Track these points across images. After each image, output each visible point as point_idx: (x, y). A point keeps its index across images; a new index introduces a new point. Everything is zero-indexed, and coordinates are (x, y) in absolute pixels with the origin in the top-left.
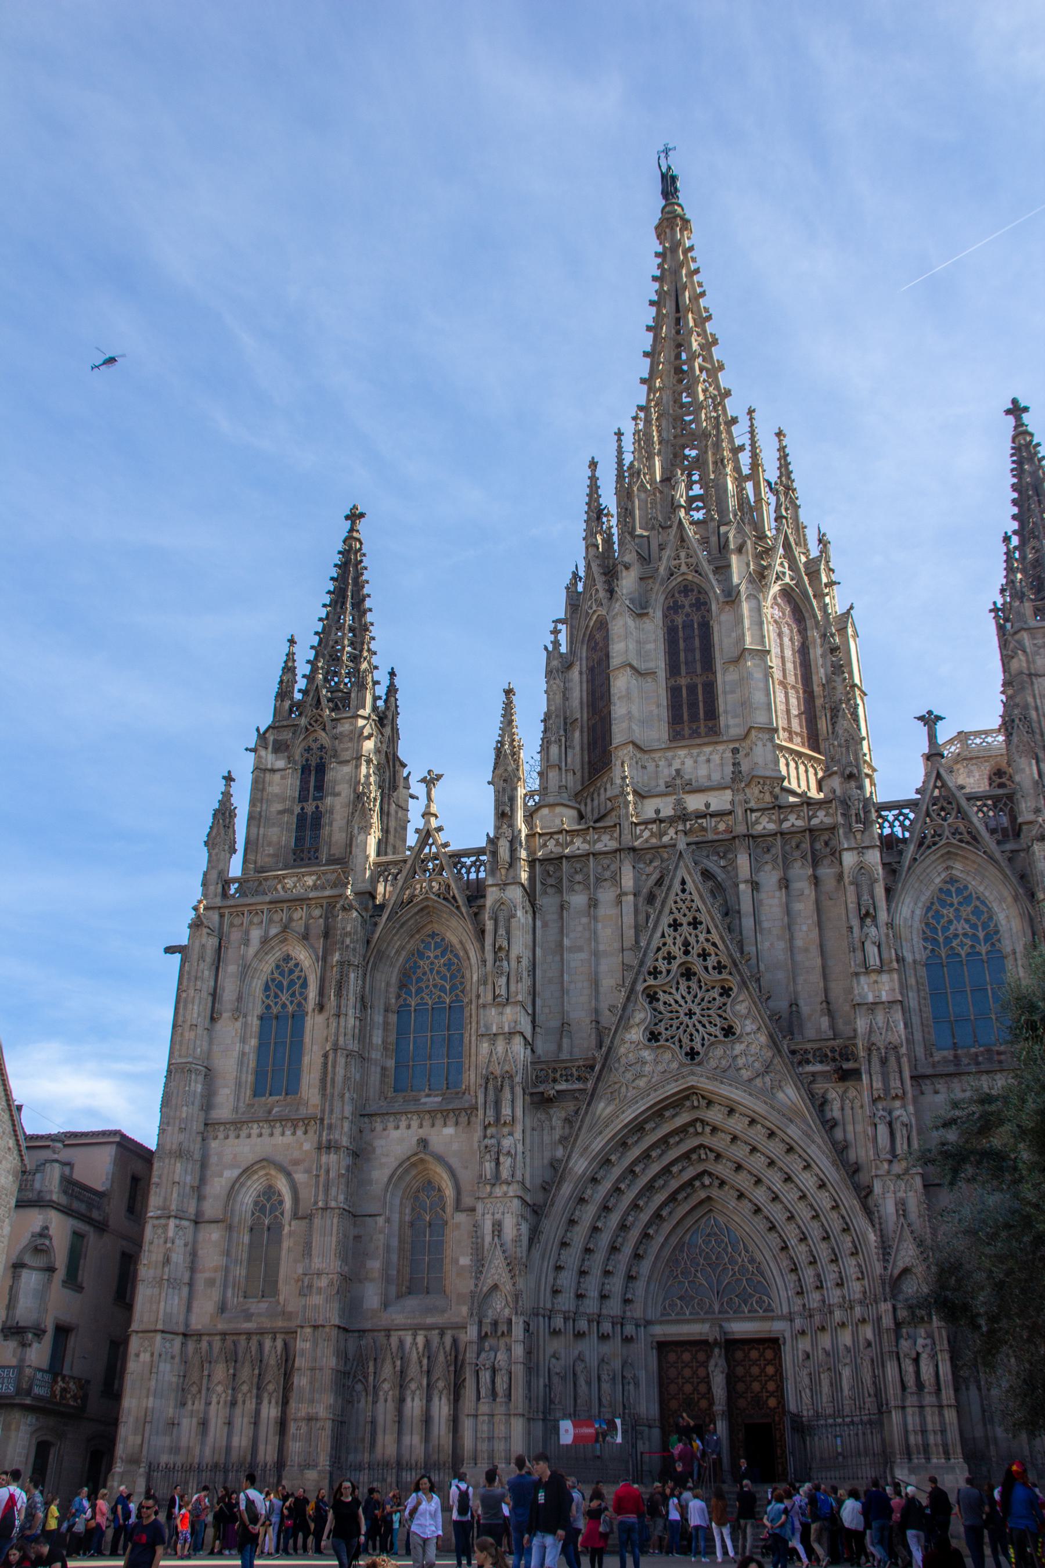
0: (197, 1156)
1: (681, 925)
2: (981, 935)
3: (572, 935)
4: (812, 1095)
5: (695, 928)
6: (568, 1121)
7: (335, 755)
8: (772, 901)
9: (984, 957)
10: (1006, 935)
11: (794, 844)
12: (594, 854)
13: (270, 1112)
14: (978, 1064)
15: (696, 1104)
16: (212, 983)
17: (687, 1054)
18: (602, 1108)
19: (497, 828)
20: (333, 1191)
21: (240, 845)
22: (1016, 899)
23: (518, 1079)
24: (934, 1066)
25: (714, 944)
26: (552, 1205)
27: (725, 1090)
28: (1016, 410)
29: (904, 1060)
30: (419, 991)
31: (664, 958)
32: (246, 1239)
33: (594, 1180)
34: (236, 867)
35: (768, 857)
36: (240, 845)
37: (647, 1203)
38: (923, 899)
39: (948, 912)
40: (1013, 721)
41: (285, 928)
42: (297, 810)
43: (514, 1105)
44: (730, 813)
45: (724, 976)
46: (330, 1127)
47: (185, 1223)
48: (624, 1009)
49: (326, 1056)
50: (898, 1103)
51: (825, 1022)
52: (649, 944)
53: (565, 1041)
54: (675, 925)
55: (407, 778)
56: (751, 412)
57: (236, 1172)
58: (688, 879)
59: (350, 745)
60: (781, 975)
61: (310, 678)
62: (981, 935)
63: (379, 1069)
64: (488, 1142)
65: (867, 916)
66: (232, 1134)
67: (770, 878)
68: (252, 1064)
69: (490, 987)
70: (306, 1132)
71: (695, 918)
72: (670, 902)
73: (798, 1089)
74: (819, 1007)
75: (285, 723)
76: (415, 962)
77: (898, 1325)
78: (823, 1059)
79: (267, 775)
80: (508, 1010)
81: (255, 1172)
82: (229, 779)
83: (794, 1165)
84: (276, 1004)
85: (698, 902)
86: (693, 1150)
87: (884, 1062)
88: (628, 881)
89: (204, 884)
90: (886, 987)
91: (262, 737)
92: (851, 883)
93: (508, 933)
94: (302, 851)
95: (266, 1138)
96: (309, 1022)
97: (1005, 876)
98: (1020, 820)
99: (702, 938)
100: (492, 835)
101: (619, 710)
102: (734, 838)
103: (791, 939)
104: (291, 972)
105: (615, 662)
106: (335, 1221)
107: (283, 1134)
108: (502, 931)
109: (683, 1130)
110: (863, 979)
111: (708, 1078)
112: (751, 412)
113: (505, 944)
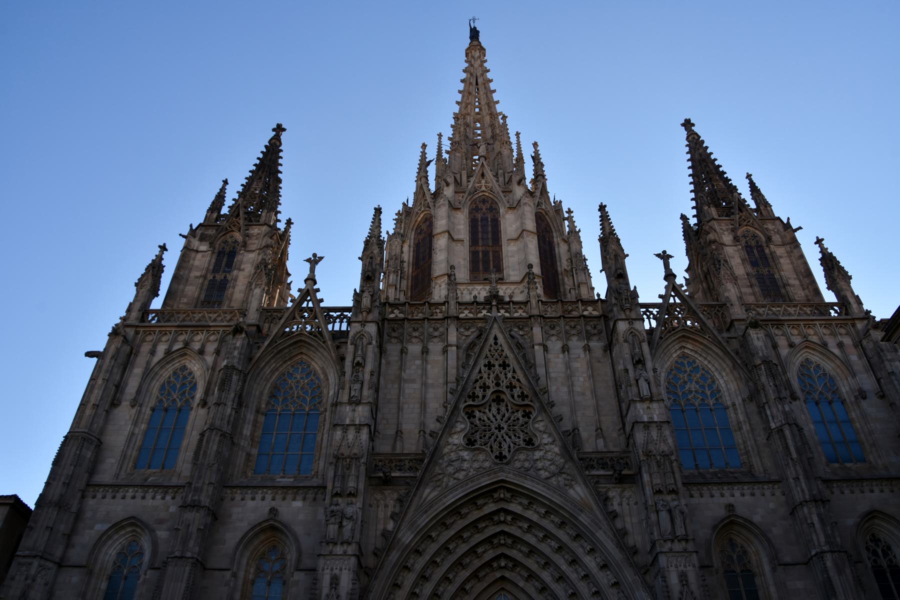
0: (74, 509)
1: (494, 366)
2: (709, 393)
3: (407, 371)
4: (598, 494)
5: (505, 369)
6: (400, 501)
7: (245, 245)
8: (557, 361)
9: (713, 408)
10: (726, 394)
11: (572, 324)
13: (146, 480)
14: (719, 478)
15: (502, 496)
16: (118, 378)
17: (496, 457)
18: (429, 493)
19: (362, 286)
20: (191, 543)
22: (734, 366)
23: (363, 460)
25: (518, 380)
26: (381, 568)
27: (528, 484)
28: (688, 124)
29: (675, 464)
30: (285, 399)
31: (481, 387)
32: (104, 586)
33: (418, 552)
34: (157, 304)
35: (553, 332)
37: (455, 577)
38: (666, 366)
39: (684, 377)
40: (719, 261)
41: (187, 344)
42: (210, 277)
43: (356, 481)
44: (526, 303)
45: (526, 402)
46: (198, 490)
47: (50, 565)
48: (449, 419)
49: (202, 435)
50: (674, 496)
52: (469, 376)
53: (398, 443)
56: (518, 134)
57: (106, 526)
61: (234, 209)
62: (709, 393)
63: (244, 454)
64: (334, 508)
65: (639, 362)
66: (109, 495)
67: (555, 345)
68: (138, 443)
69: (347, 391)
70: (173, 498)
71: (504, 362)
72: (486, 351)
73: (587, 487)
74: (594, 433)
78: (604, 466)
79: (193, 254)
80: (360, 408)
81: (123, 527)
82: (163, 248)
83: (578, 549)
84: (168, 400)
85: (507, 352)
86: (495, 535)
87: (659, 464)
89: (129, 310)
90: (657, 412)
91: (193, 232)
92: (626, 341)
95: (138, 500)
96: (193, 413)
97: (726, 353)
98: (733, 318)
99: (509, 375)
100: (358, 291)
102: (530, 317)
103: (573, 385)
104: (185, 377)
105: (435, 232)
106: (188, 569)
107: (153, 498)
108: (360, 352)
109: (489, 517)
110: (638, 405)
111: (515, 475)
112: (518, 134)
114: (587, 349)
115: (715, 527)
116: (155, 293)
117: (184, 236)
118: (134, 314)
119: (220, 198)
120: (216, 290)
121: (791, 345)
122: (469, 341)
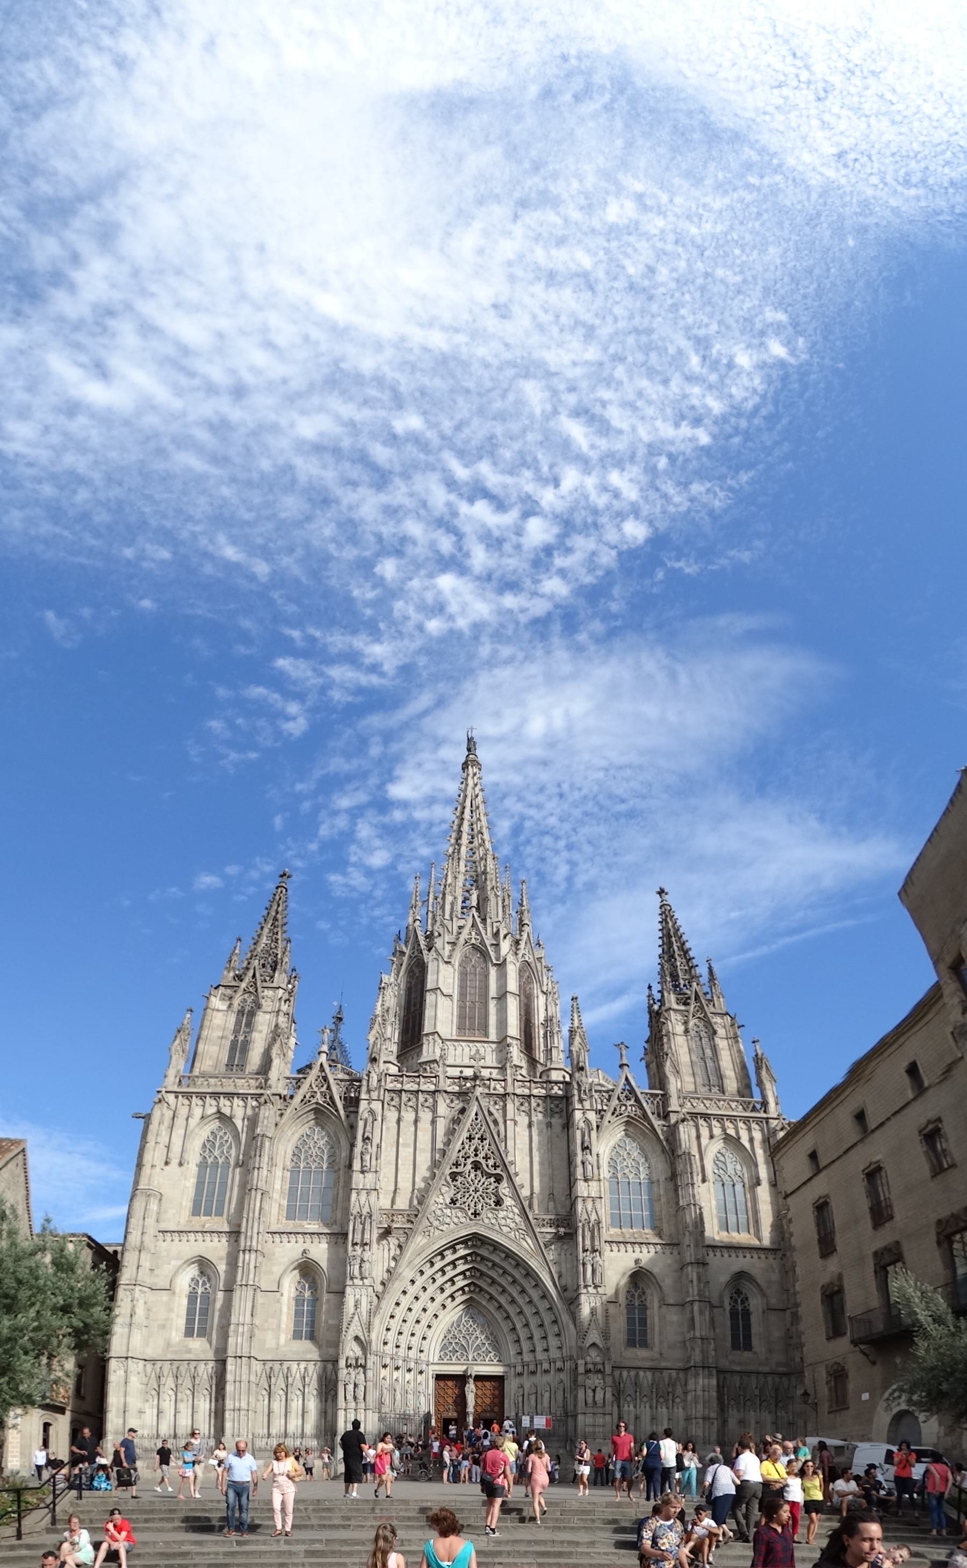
18: (419, 1241)
22: (664, 1150)
24: (611, 1236)
30: (306, 1158)
35: (522, 1108)
45: (498, 1171)
51: (551, 1204)
53: (398, 1200)
54: (470, 1138)
58: (480, 1113)
60: (528, 1176)
67: (523, 1120)
77: (588, 1371)
101: (428, 1013)
105: (429, 986)
114: (549, 1125)
115: (624, 1274)
121: (712, 1137)
122: (454, 1113)
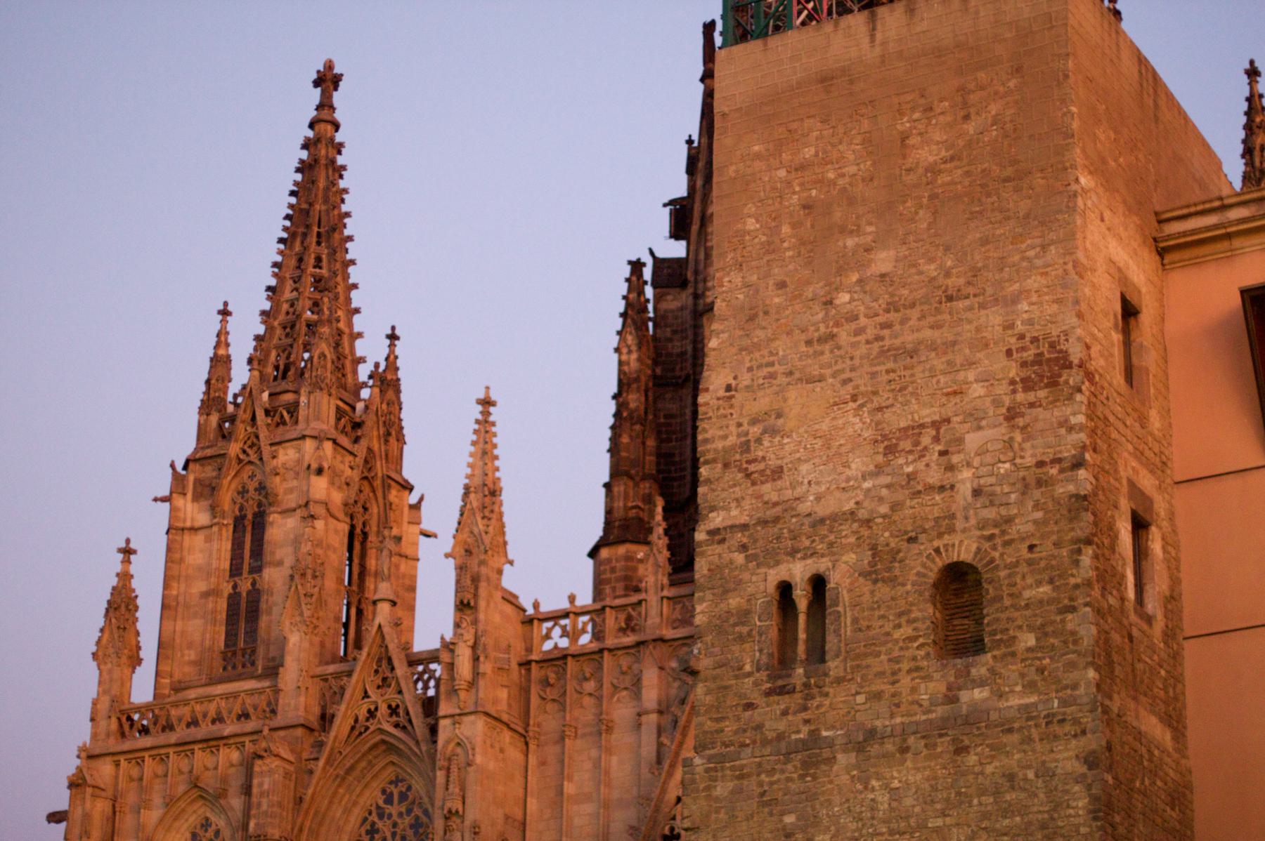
12: (610, 650)
19: (457, 625)
21: (149, 651)
36: (149, 651)
42: (227, 589)
55: (416, 507)
59: (295, 483)
75: (209, 452)
76: (373, 824)
79: (187, 539)
82: (127, 552)
88: (651, 696)
89: (92, 720)
91: (178, 481)
93: (463, 789)
94: (234, 653)
113: (456, 805)
116: (136, 661)
117: (164, 500)
118: (103, 724)
119: (220, 363)
120: (244, 613)
